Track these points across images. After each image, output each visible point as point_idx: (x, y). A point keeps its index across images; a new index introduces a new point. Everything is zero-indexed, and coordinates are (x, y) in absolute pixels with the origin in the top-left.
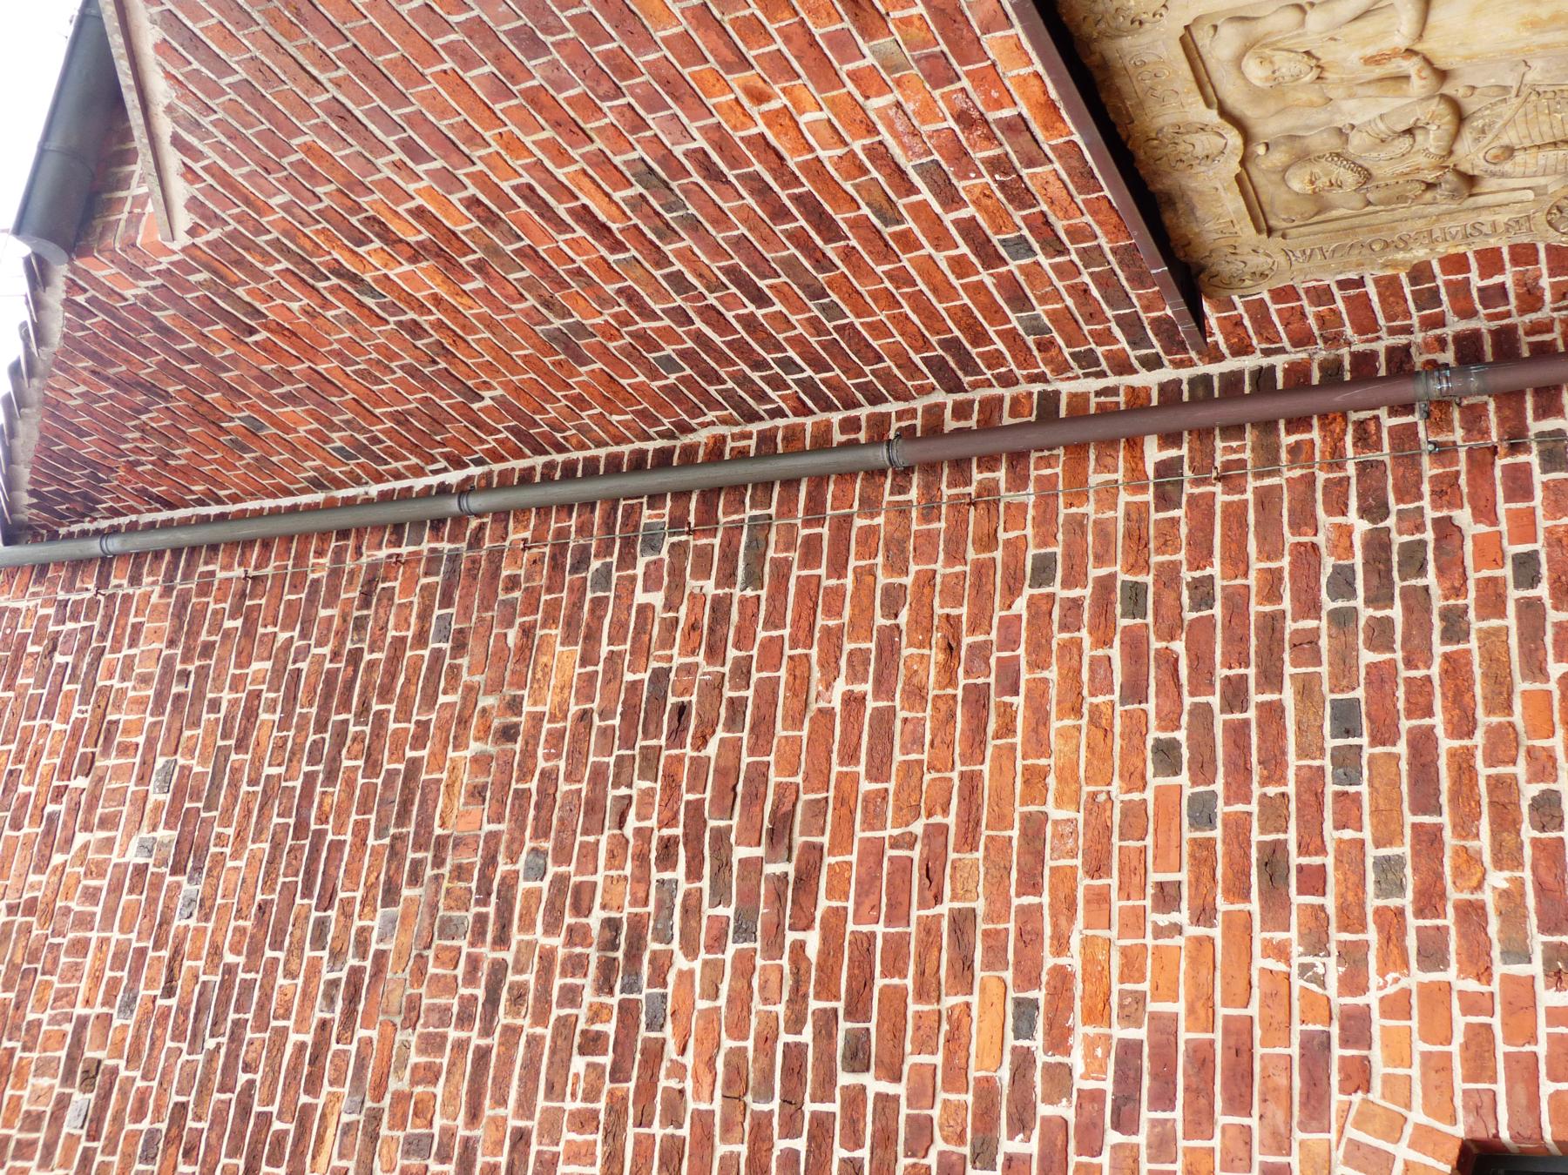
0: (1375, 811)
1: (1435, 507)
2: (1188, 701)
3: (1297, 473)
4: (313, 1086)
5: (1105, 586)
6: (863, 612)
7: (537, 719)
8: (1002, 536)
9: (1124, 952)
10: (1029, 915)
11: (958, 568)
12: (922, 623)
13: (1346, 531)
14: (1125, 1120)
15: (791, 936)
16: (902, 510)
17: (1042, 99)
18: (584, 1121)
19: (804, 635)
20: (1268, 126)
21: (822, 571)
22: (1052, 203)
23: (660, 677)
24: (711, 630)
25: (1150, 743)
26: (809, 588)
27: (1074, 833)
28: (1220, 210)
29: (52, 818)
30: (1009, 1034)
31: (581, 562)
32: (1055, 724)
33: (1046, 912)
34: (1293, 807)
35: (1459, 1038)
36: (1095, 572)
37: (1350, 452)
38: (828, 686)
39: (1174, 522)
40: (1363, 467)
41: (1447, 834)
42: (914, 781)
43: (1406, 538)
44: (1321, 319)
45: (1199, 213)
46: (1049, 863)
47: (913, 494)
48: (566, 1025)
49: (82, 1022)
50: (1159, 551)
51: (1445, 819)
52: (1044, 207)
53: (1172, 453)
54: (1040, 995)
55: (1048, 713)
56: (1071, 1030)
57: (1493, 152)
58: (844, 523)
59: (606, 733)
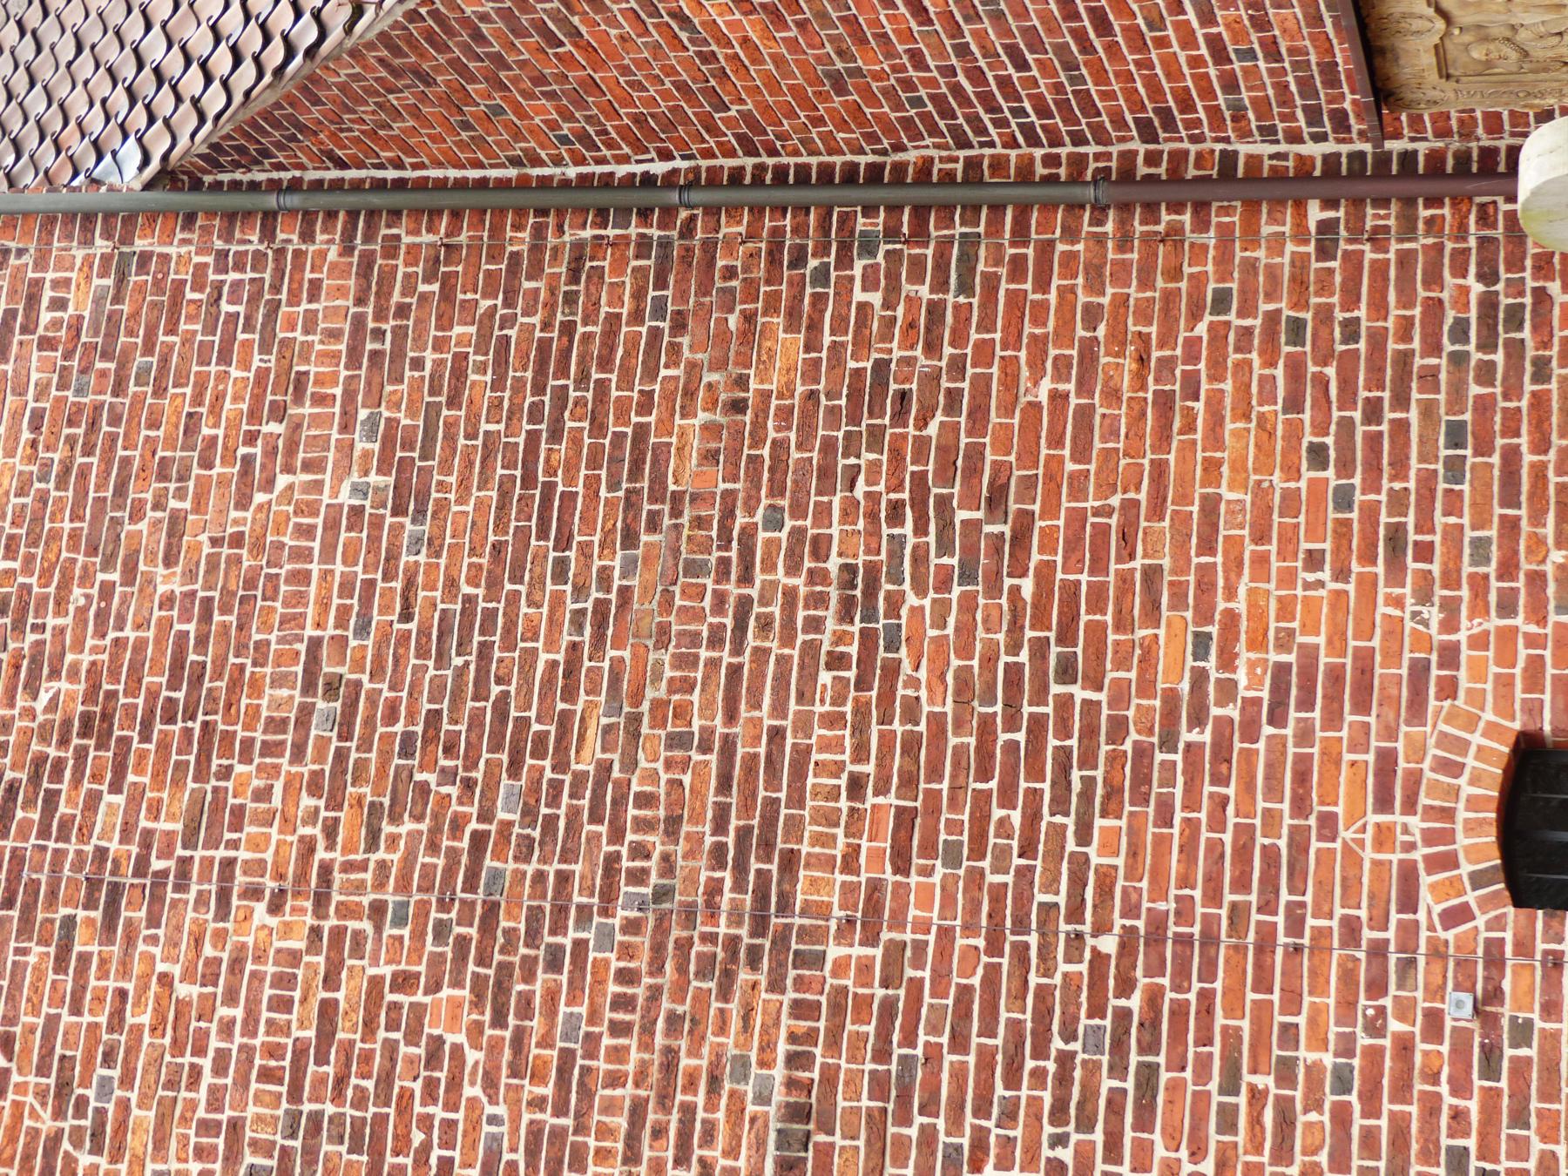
0: (1473, 504)
1: (1535, 278)
2: (1336, 414)
3: (1430, 241)
4: (570, 694)
5: (1273, 318)
6: (1066, 323)
7: (765, 396)
8: (1187, 270)
9: (1280, 599)
10: (1206, 572)
11: (1149, 294)
12: (1118, 337)
13: (1465, 290)
14: (1277, 718)
15: (1008, 582)
16: (1100, 240)
20: (1464, 17)
21: (1028, 286)
23: (881, 367)
24: (928, 330)
25: (1305, 445)
26: (1015, 299)
27: (1243, 510)
29: (248, 461)
30: (1189, 658)
31: (799, 260)
32: (1229, 426)
33: (1220, 569)
34: (1413, 498)
35: (1521, 664)
36: (1264, 307)
37: (1472, 228)
38: (1036, 383)
39: (1331, 271)
40: (1482, 241)
41: (1524, 523)
42: (1112, 465)
43: (1511, 301)
46: (1222, 532)
47: (1109, 227)
48: (811, 649)
49: (315, 644)
50: (1317, 294)
51: (1523, 512)
53: (1331, 214)
54: (1214, 630)
55: (1223, 418)
56: (1237, 655)
58: (1046, 248)
59: (833, 412)
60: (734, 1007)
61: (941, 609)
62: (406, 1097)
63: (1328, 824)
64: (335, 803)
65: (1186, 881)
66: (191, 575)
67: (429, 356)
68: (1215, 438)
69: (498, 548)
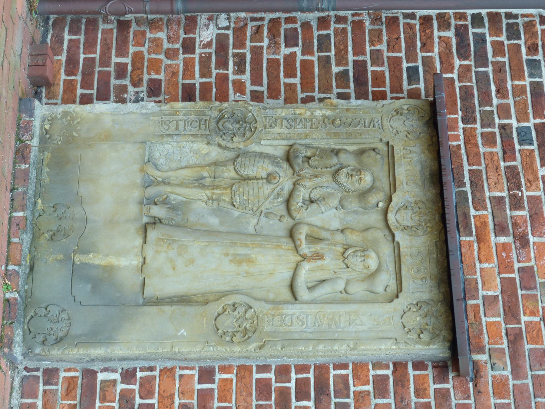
17: (482, 245)
20: (375, 218)
22: (497, 168)
28: (409, 167)
44: (380, 40)
45: (419, 167)
52: (502, 164)
57: (276, 181)
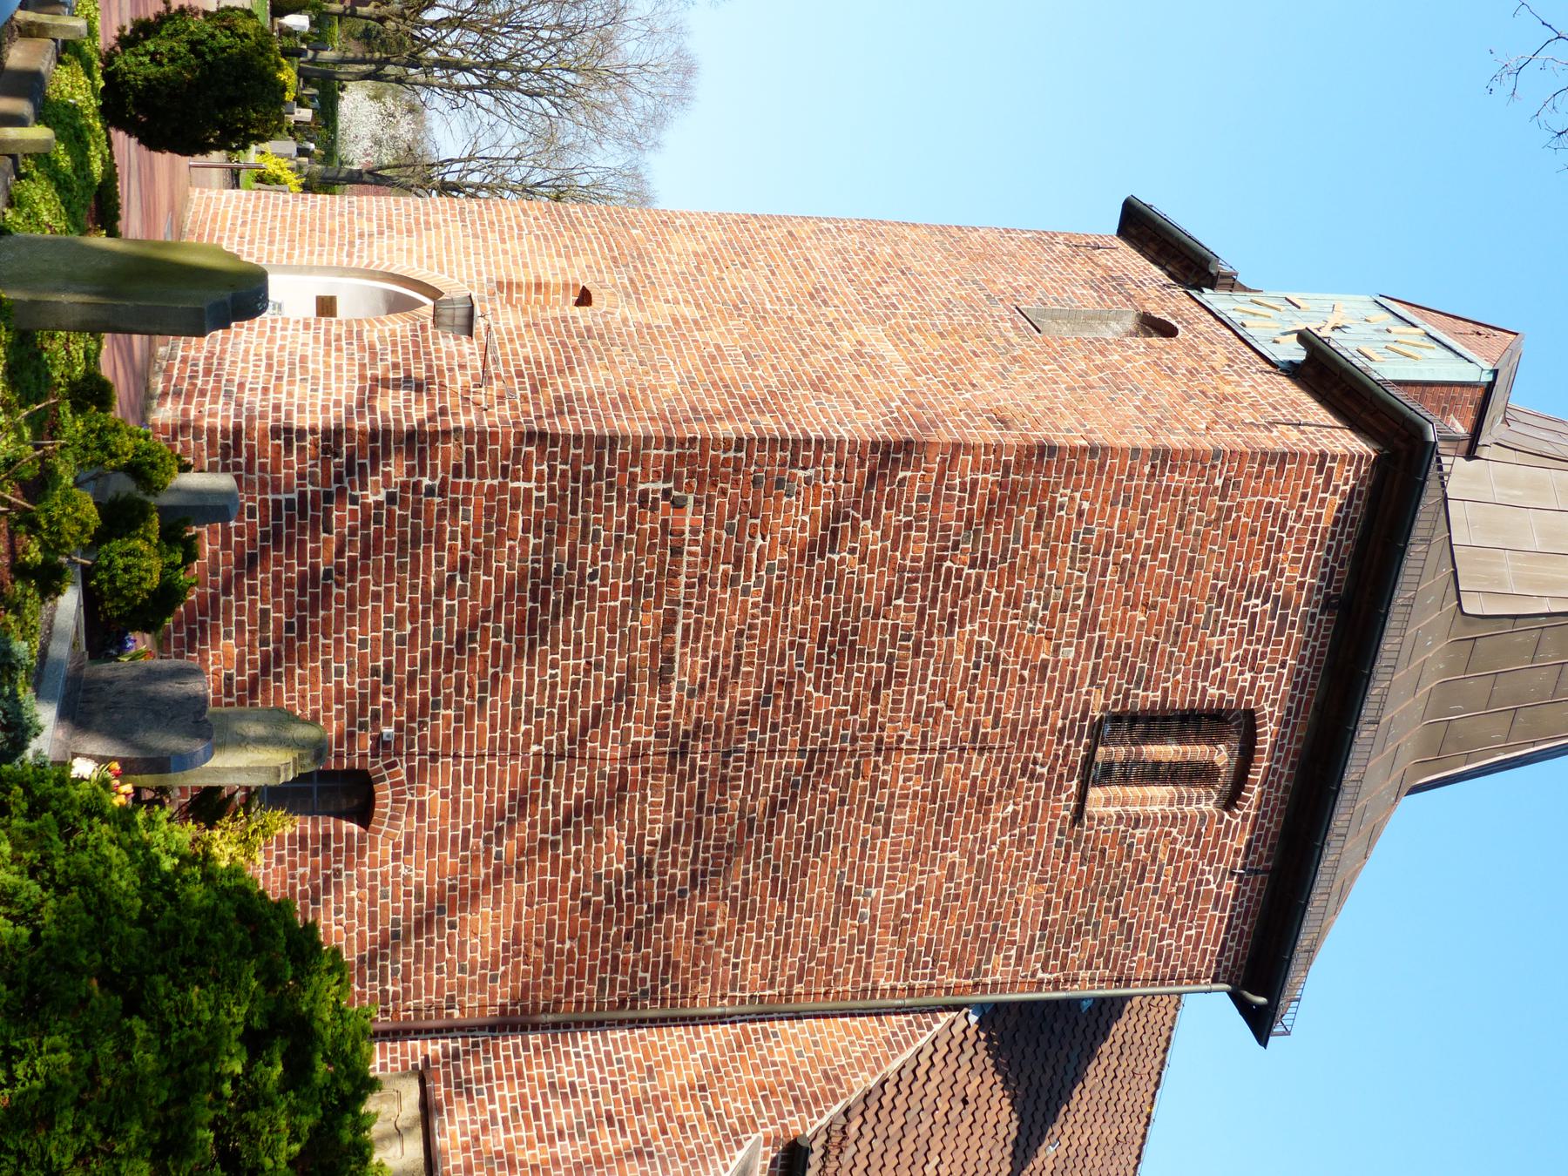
5: (473, 973)
14: (466, 832)
18: (652, 822)
19: (581, 963)
26: (581, 975)
29: (918, 902)
60: (694, 715)
61: (609, 863)
62: (839, 671)
63: (444, 795)
64: (874, 780)
65: (503, 772)
66: (943, 859)
67: (837, 945)
68: (495, 931)
69: (804, 874)
